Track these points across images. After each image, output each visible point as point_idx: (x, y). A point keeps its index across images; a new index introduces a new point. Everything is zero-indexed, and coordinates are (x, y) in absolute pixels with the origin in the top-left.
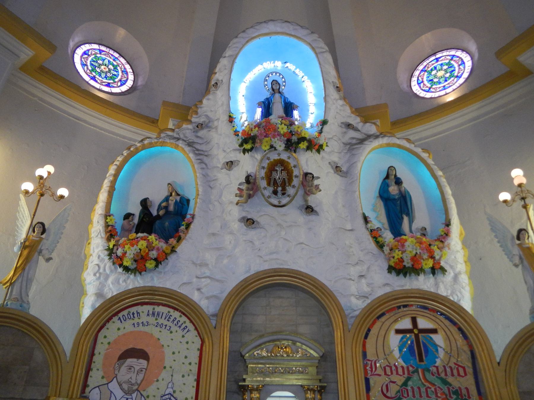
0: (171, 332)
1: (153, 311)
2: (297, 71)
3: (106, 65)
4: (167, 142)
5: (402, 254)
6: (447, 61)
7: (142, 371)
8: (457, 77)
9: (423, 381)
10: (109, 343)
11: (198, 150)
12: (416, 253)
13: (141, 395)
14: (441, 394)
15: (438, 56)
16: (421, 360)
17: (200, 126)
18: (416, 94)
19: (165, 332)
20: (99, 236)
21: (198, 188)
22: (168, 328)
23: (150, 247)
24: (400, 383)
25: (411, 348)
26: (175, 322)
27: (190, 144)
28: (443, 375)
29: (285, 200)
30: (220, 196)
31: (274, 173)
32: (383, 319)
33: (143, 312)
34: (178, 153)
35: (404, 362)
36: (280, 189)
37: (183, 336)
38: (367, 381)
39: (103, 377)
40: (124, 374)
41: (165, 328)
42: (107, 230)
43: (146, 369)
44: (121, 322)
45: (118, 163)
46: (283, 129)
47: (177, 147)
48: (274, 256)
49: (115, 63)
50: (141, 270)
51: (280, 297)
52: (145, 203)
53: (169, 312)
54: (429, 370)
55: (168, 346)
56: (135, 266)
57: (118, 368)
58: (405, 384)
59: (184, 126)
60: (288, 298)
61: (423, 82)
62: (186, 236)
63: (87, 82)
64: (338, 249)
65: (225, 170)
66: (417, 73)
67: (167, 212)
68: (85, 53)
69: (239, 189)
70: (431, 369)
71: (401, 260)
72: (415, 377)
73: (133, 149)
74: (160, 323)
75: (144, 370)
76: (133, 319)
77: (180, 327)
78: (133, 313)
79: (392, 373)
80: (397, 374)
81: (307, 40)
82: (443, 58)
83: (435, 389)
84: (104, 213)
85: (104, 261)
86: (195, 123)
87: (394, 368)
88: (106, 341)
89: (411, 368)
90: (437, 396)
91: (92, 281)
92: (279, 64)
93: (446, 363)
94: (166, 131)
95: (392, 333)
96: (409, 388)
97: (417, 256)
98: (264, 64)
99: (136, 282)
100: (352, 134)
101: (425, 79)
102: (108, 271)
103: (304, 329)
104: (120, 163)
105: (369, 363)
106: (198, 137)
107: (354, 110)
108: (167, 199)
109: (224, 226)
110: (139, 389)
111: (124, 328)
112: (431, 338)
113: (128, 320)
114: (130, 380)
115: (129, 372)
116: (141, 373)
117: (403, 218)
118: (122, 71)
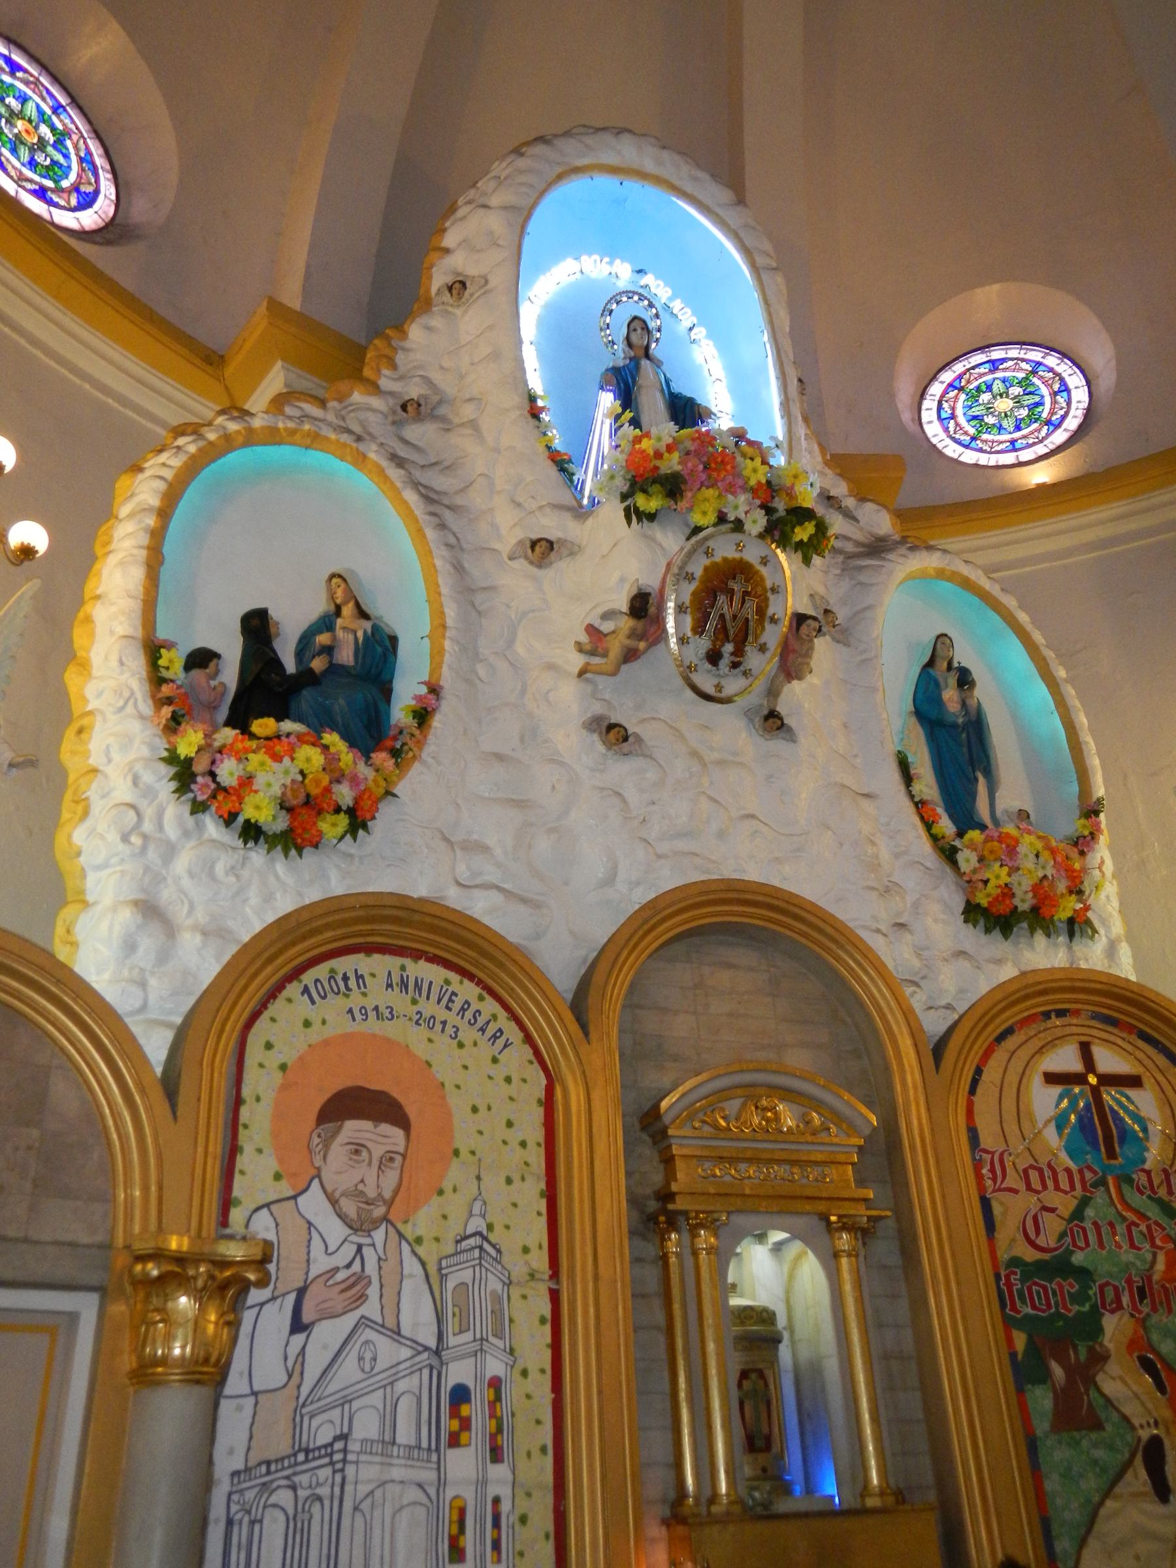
0: (461, 1045)
1: (402, 976)
2: (676, 306)
3: (30, 121)
4: (327, 438)
5: (1009, 875)
6: (1021, 375)
7: (391, 1159)
8: (1048, 422)
9: (1119, 1206)
10: (283, 1067)
12: (1045, 877)
13: (401, 1235)
14: (1164, 1240)
15: (997, 354)
16: (1112, 1154)
17: (411, 409)
18: (934, 446)
19: (444, 1042)
20: (130, 709)
21: (442, 606)
22: (449, 1030)
24: (1066, 1214)
25: (1085, 1125)
26: (469, 1015)
28: (1162, 1192)
29: (733, 684)
30: (511, 642)
31: (722, 599)
32: (1011, 1043)
33: (373, 975)
34: (361, 483)
35: (1072, 1158)
36: (729, 648)
37: (495, 1060)
38: (986, 1204)
39: (278, 1177)
41: (443, 1031)
42: (160, 695)
43: (404, 1156)
44: (313, 1002)
45: (169, 474)
47: (360, 460)
48: (681, 845)
50: (303, 840)
51: (730, 966)
53: (447, 982)
54: (1130, 1181)
55: (458, 1087)
56: (281, 824)
57: (320, 1146)
58: (1078, 1214)
59: (357, 397)
60: (751, 969)
61: (953, 417)
62: (421, 749)
64: (841, 844)
65: (522, 560)
66: (936, 389)
69: (591, 630)
70: (1134, 1176)
71: (1007, 892)
72: (1100, 1197)
73: (218, 438)
74: (427, 1014)
75: (399, 1159)
76: (347, 996)
77: (483, 1030)
78: (345, 974)
79: (1045, 1187)
80: (1057, 1188)
81: (731, 223)
82: (1010, 363)
83: (1149, 1228)
84: (139, 633)
85: (156, 797)
86: (391, 394)
87: (1047, 1173)
88: (274, 1059)
89: (1088, 1175)
90: (1153, 1245)
91: (114, 860)
93: (1169, 1163)
94: (299, 400)
95: (1037, 1081)
96: (1088, 1225)
97: (1046, 883)
98: (584, 258)
99: (272, 879)
101: (959, 411)
102: (172, 831)
103: (798, 1059)
104: (176, 476)
105: (987, 1157)
107: (828, 457)
108: (326, 623)
109: (531, 734)
110: (391, 1217)
111: (324, 1022)
112: (1128, 1098)
113: (330, 995)
114: (361, 1187)
115: (355, 1161)
116: (391, 1168)
117: (976, 780)
118: (81, 160)
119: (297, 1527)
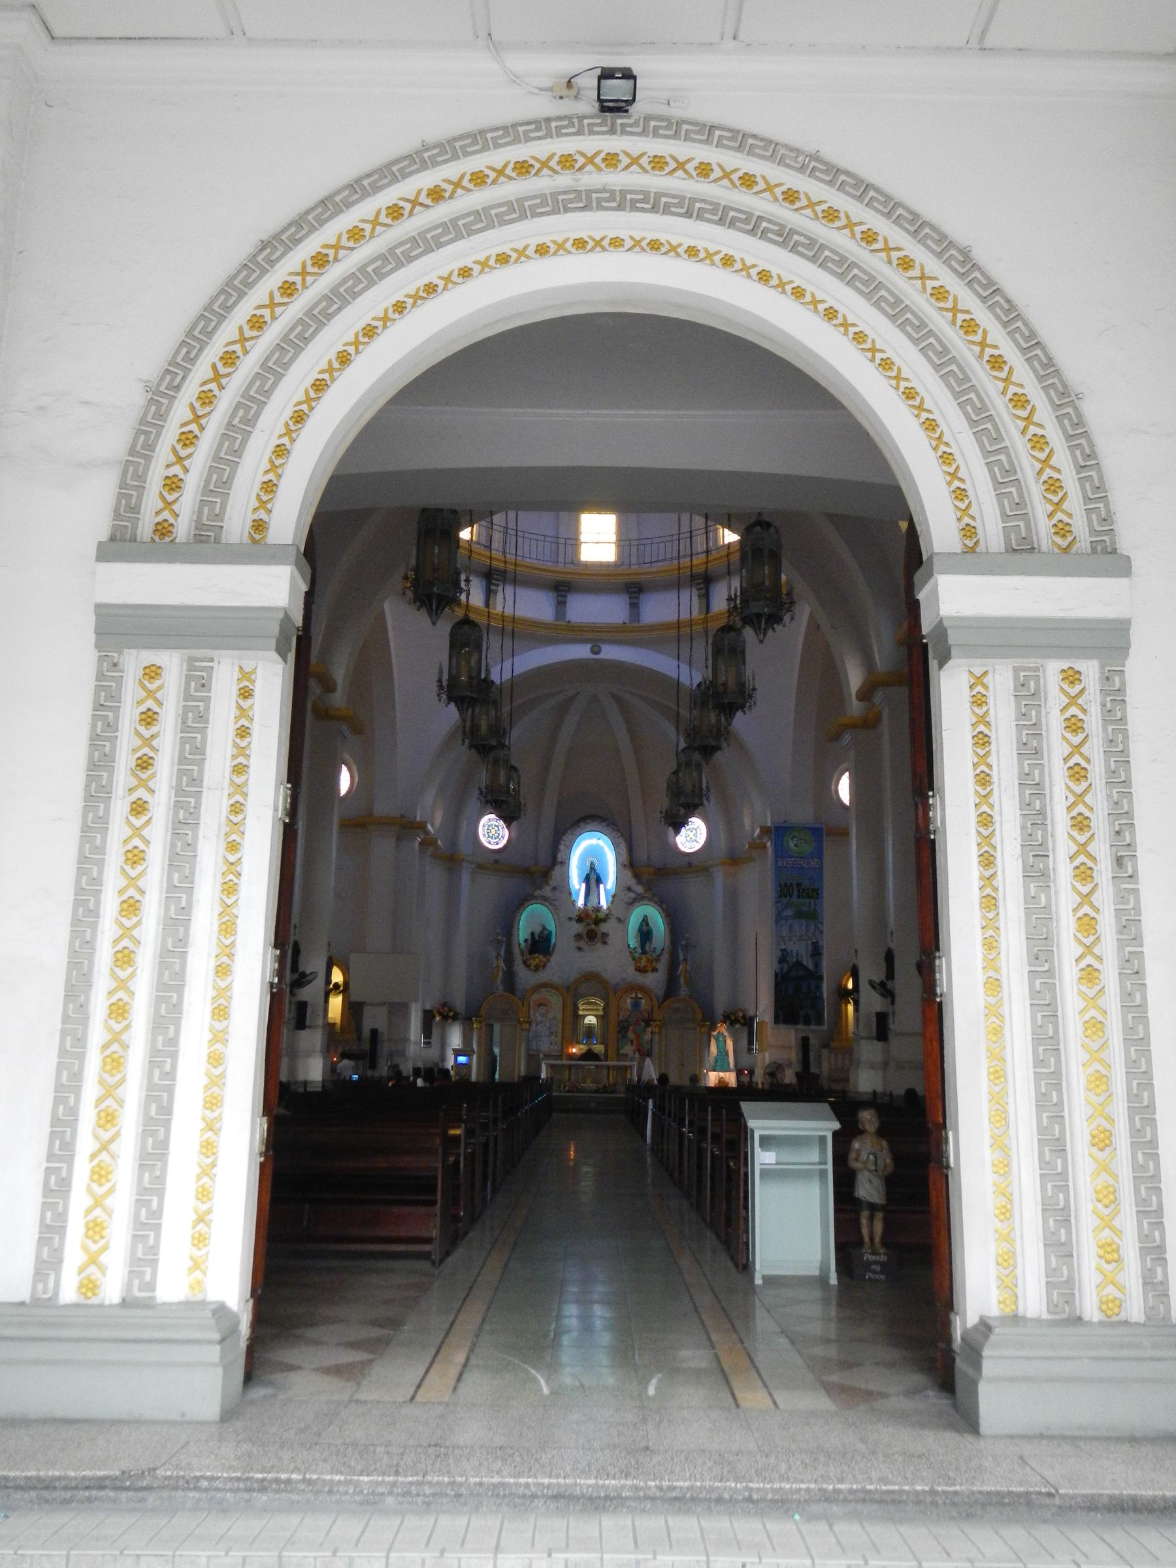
17: (554, 889)
23: (541, 961)
46: (594, 916)
52: (532, 934)
92: (594, 841)
100: (632, 895)
108: (542, 932)
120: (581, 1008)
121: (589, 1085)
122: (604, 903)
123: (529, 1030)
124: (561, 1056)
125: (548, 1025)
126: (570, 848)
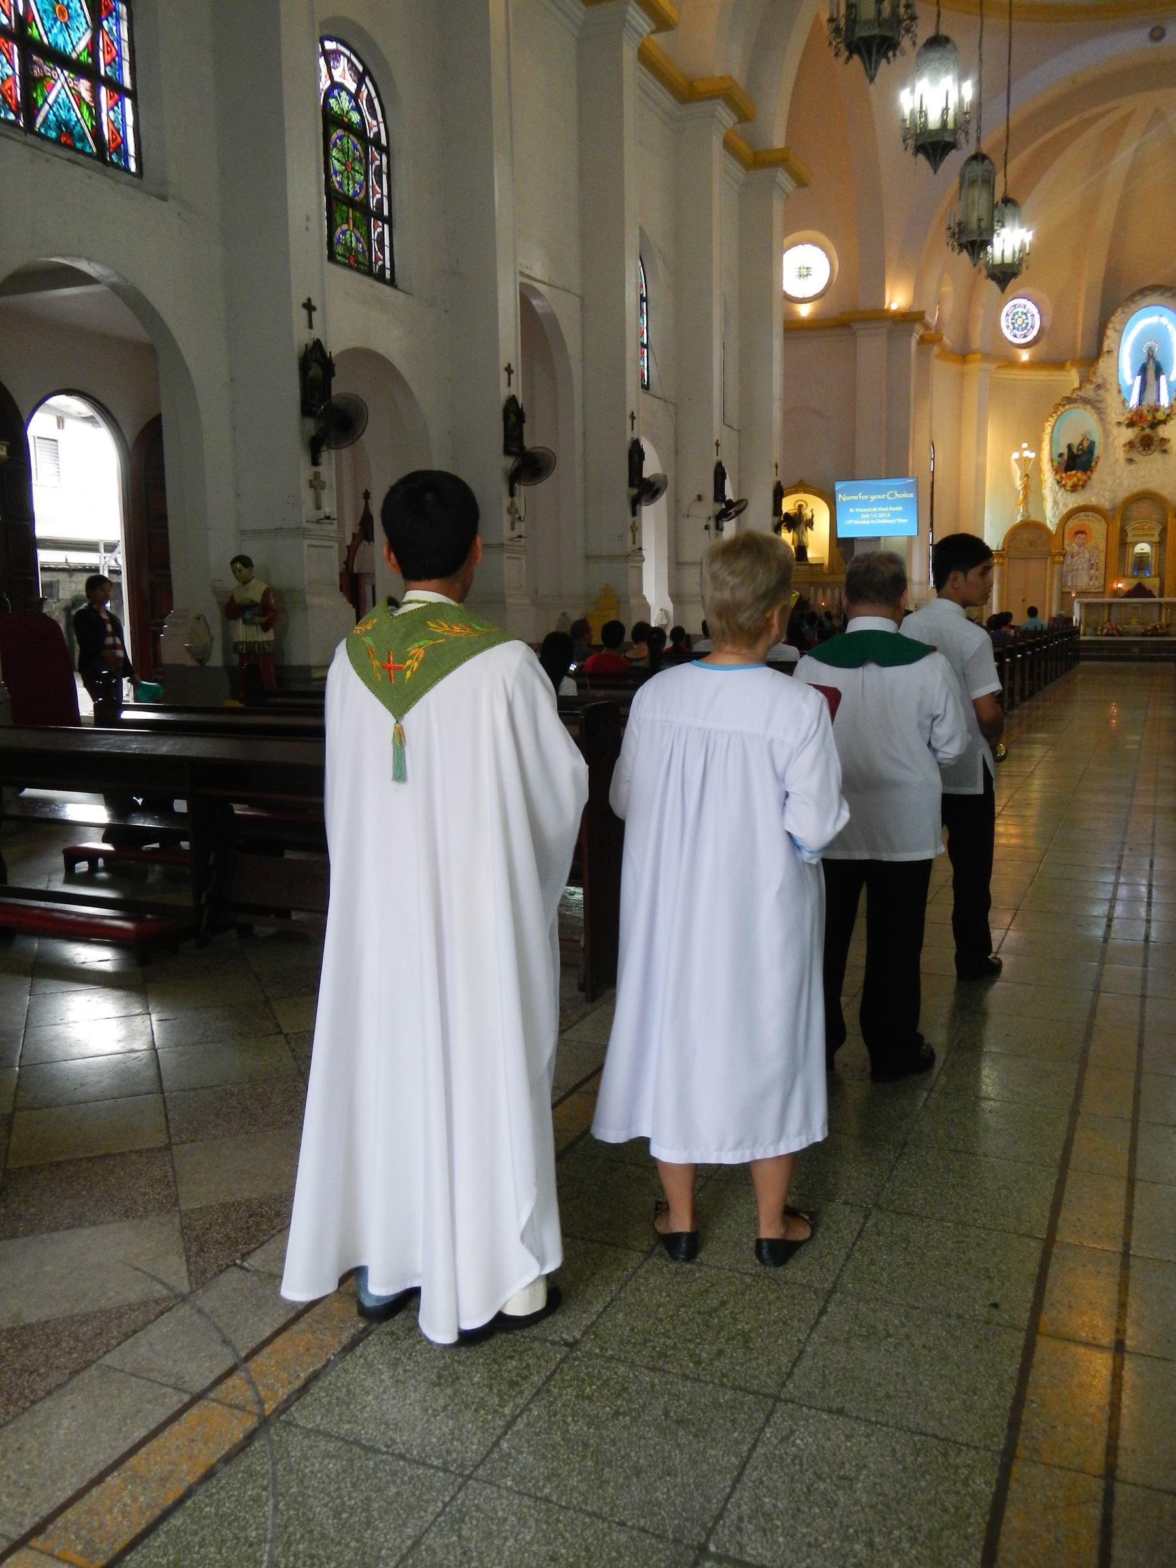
11: (1099, 409)
17: (1099, 387)
27: (1094, 407)
40: (1077, 540)
46: (1150, 418)
49: (1025, 311)
52: (1069, 447)
59: (1088, 386)
63: (1011, 343)
67: (1084, 452)
68: (1007, 315)
92: (1154, 320)
103: (1155, 517)
106: (1098, 395)
108: (1081, 444)
109: (1116, 462)
119: (1073, 576)
120: (1130, 534)
121: (1134, 625)
122: (1165, 401)
123: (1063, 562)
124: (1103, 592)
125: (1087, 555)
126: (1120, 333)
